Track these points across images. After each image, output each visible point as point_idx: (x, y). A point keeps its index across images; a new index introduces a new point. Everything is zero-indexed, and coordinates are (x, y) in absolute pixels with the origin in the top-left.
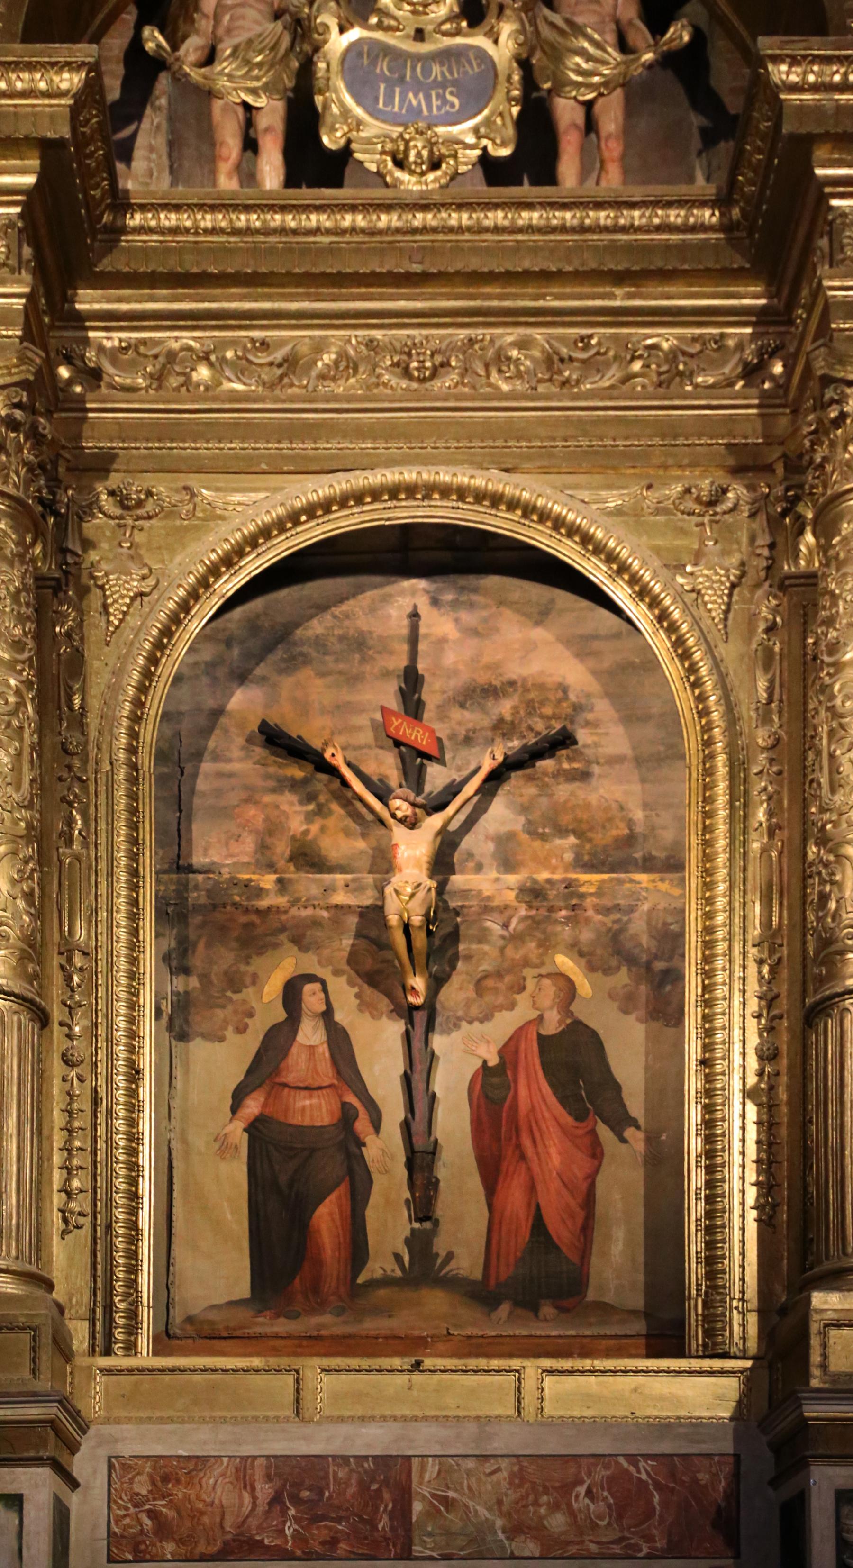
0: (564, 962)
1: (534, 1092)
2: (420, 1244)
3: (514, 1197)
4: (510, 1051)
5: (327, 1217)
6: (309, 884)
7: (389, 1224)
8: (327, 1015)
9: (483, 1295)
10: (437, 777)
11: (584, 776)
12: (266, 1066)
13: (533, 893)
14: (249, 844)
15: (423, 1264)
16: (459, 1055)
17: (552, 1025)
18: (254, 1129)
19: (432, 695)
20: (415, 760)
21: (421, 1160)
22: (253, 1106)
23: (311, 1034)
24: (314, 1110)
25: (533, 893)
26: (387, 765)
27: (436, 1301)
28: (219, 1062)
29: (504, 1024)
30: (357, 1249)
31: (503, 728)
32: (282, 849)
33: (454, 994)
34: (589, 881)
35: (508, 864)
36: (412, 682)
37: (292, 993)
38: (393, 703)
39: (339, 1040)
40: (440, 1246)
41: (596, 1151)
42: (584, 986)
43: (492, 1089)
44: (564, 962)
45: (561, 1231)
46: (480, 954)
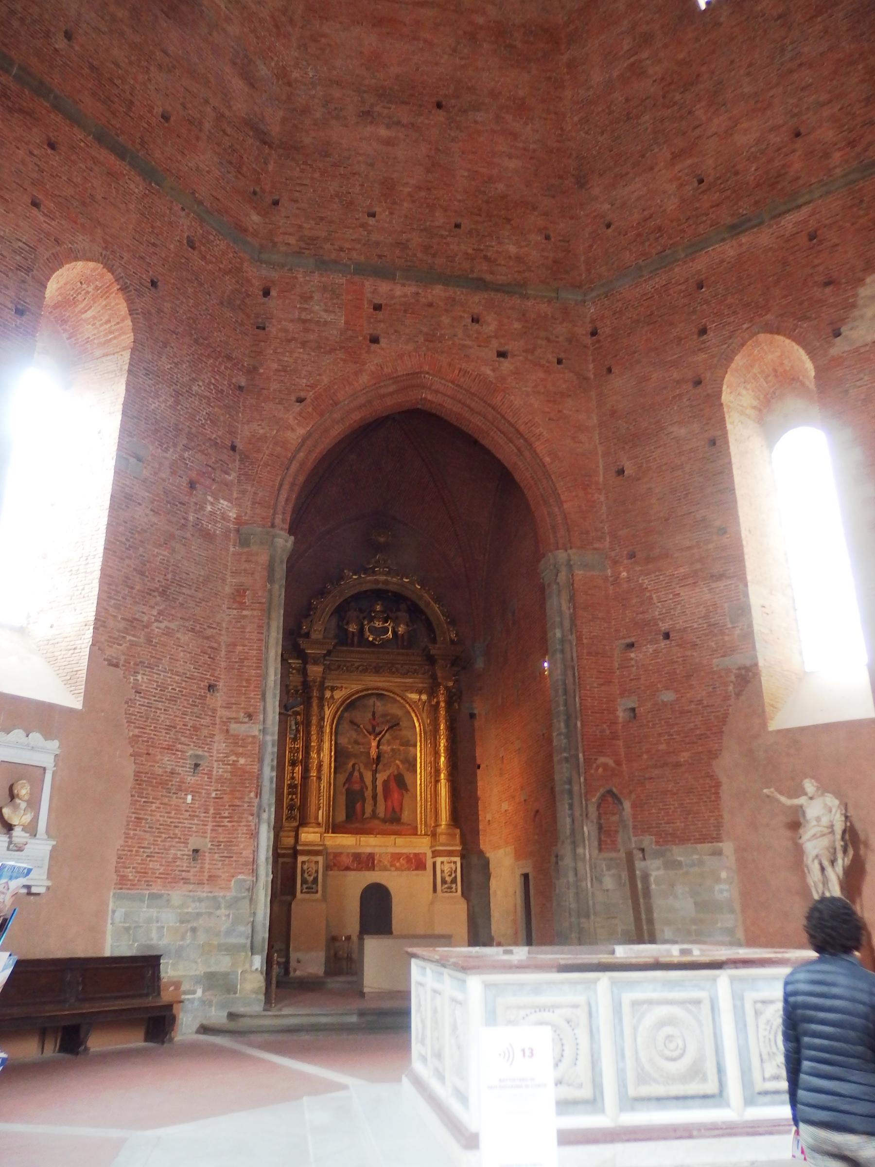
0: (397, 762)
1: (393, 785)
2: (374, 811)
3: (389, 803)
4: (389, 777)
5: (358, 806)
6: (357, 747)
7: (369, 810)
8: (359, 770)
9: (384, 821)
10: (378, 729)
11: (400, 730)
12: (349, 780)
13: (393, 750)
14: (346, 740)
15: (374, 815)
16: (381, 777)
17: (396, 773)
18: (347, 790)
19: (377, 715)
20: (374, 727)
21: (375, 797)
22: (347, 786)
23: (356, 774)
24: (356, 787)
25: (393, 750)
26: (371, 729)
27: (376, 822)
28: (342, 778)
29: (388, 773)
30: (363, 813)
31: (388, 721)
32: (352, 740)
33: (380, 767)
34: (402, 748)
35: (389, 744)
36: (374, 714)
37: (354, 765)
38: (370, 716)
39: (361, 775)
40: (377, 811)
41: (403, 795)
42: (401, 766)
43: (386, 783)
44: (397, 762)
45: (397, 809)
46: (384, 760)
